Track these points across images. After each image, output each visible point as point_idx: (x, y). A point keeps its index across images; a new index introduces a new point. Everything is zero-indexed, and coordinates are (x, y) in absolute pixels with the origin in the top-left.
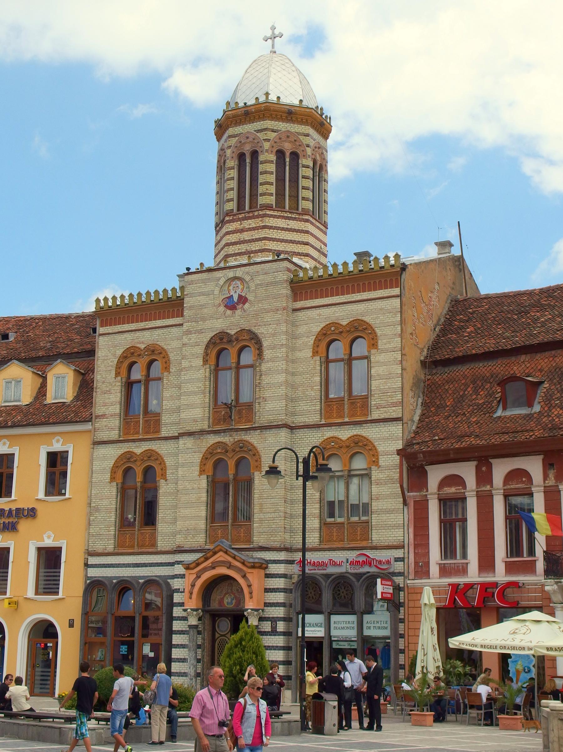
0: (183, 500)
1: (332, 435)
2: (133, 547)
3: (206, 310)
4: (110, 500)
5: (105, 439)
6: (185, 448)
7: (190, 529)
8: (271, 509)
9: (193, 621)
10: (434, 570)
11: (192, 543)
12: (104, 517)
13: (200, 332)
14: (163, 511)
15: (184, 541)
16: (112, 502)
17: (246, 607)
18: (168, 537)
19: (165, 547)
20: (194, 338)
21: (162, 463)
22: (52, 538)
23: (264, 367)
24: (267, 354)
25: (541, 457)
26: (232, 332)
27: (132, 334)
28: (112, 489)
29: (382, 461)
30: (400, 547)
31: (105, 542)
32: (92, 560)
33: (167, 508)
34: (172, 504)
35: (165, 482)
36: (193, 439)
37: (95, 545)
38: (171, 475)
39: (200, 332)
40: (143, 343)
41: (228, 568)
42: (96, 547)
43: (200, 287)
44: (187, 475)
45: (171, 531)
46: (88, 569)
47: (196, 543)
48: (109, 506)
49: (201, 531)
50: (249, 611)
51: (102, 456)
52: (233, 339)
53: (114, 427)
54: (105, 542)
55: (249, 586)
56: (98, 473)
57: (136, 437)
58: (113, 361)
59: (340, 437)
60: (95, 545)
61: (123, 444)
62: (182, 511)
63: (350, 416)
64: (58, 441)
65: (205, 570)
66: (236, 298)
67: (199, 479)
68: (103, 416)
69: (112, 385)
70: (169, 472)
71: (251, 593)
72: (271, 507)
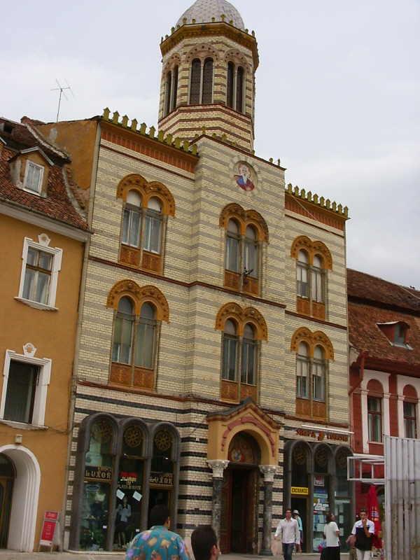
1: (305, 326)
2: (125, 383)
5: (103, 258)
9: (218, 474)
10: (366, 447)
13: (218, 194)
20: (212, 197)
21: (164, 304)
22: (33, 352)
23: (270, 250)
24: (272, 240)
26: (245, 209)
29: (336, 355)
30: (345, 427)
32: (81, 390)
39: (218, 194)
40: (149, 176)
41: (255, 425)
46: (77, 399)
52: (246, 214)
57: (133, 266)
58: (115, 180)
63: (314, 315)
64: (44, 239)
65: (234, 424)
66: (245, 181)
68: (101, 232)
70: (171, 315)
71: (273, 452)
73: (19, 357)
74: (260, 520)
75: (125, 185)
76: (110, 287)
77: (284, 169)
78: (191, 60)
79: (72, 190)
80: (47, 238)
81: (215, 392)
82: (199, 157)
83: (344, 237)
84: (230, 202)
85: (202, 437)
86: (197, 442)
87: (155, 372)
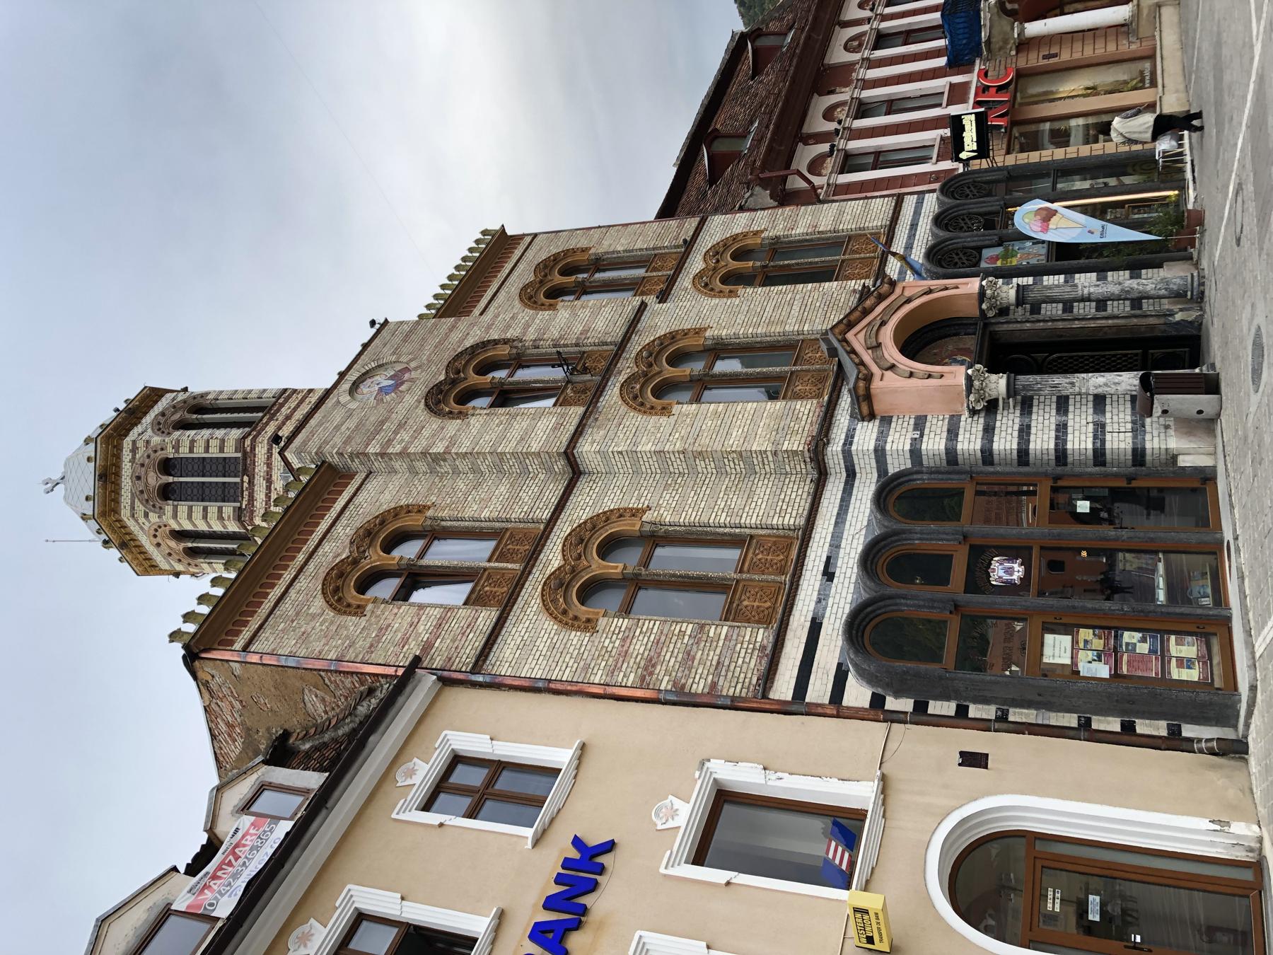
0: (707, 440)
3: (372, 419)
4: (637, 634)
6: (601, 441)
7: (776, 427)
8: (785, 309)
9: (998, 384)
11: (809, 421)
12: (676, 651)
14: (714, 514)
15: (799, 436)
16: (644, 630)
17: (977, 313)
18: (780, 504)
19: (801, 509)
22: (678, 803)
25: (816, 96)
26: (442, 377)
27: (302, 577)
28: (612, 629)
31: (743, 651)
32: (784, 688)
33: (712, 506)
34: (706, 496)
35: (651, 512)
36: (590, 430)
37: (741, 680)
38: (643, 499)
41: (883, 323)
42: (749, 675)
43: (325, 429)
44: (659, 435)
45: (766, 497)
47: (811, 415)
48: (653, 636)
49: (788, 407)
50: (984, 306)
51: (519, 651)
53: (470, 619)
54: (743, 651)
55: (930, 291)
56: (554, 664)
59: (698, 271)
60: (741, 680)
61: (520, 598)
62: (731, 442)
66: (391, 382)
67: (676, 417)
69: (371, 625)
72: (779, 311)
73: (684, 841)
74: (1112, 308)
75: (339, 600)
76: (550, 625)
77: (386, 320)
78: (159, 503)
79: (336, 727)
80: (410, 765)
81: (806, 411)
82: (324, 462)
83: (535, 235)
84: (422, 405)
85: (911, 427)
86: (922, 436)
87: (753, 532)
